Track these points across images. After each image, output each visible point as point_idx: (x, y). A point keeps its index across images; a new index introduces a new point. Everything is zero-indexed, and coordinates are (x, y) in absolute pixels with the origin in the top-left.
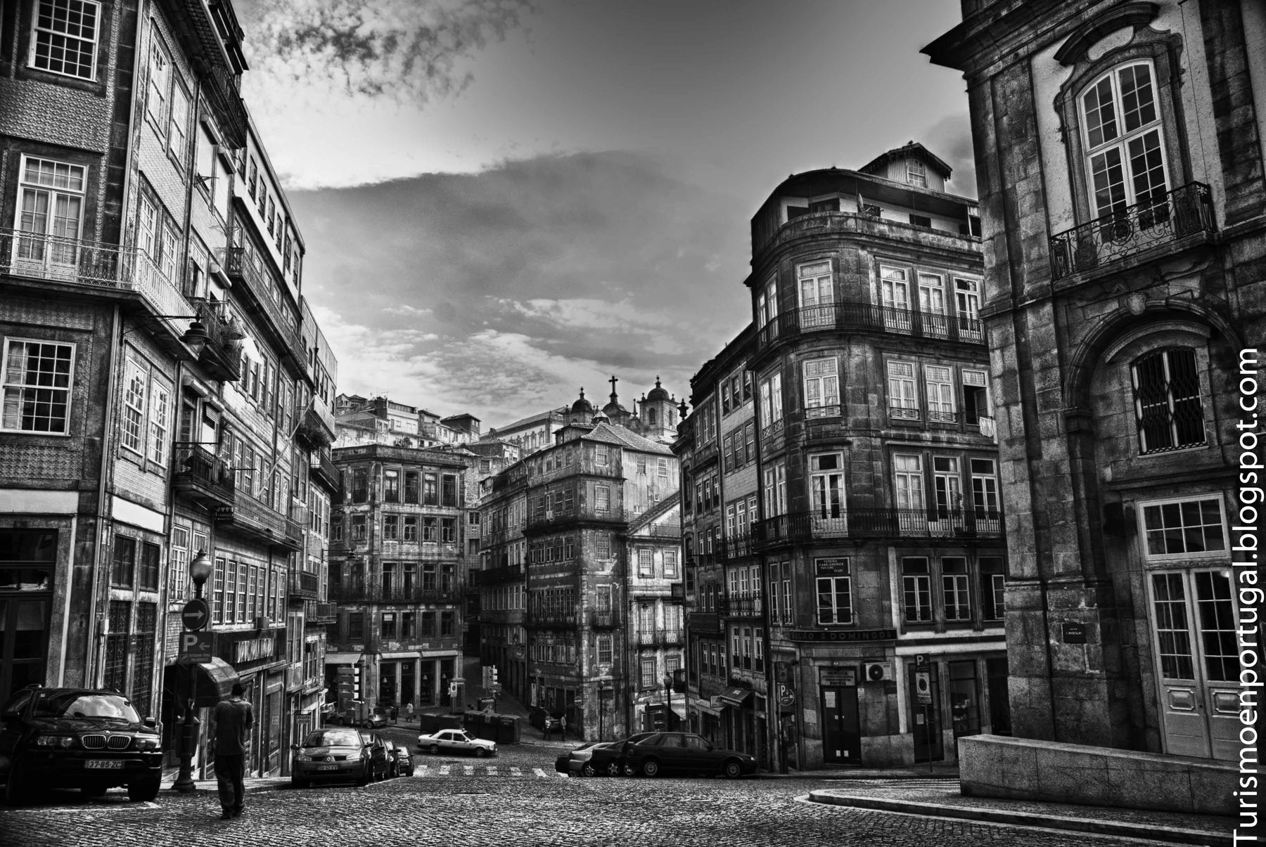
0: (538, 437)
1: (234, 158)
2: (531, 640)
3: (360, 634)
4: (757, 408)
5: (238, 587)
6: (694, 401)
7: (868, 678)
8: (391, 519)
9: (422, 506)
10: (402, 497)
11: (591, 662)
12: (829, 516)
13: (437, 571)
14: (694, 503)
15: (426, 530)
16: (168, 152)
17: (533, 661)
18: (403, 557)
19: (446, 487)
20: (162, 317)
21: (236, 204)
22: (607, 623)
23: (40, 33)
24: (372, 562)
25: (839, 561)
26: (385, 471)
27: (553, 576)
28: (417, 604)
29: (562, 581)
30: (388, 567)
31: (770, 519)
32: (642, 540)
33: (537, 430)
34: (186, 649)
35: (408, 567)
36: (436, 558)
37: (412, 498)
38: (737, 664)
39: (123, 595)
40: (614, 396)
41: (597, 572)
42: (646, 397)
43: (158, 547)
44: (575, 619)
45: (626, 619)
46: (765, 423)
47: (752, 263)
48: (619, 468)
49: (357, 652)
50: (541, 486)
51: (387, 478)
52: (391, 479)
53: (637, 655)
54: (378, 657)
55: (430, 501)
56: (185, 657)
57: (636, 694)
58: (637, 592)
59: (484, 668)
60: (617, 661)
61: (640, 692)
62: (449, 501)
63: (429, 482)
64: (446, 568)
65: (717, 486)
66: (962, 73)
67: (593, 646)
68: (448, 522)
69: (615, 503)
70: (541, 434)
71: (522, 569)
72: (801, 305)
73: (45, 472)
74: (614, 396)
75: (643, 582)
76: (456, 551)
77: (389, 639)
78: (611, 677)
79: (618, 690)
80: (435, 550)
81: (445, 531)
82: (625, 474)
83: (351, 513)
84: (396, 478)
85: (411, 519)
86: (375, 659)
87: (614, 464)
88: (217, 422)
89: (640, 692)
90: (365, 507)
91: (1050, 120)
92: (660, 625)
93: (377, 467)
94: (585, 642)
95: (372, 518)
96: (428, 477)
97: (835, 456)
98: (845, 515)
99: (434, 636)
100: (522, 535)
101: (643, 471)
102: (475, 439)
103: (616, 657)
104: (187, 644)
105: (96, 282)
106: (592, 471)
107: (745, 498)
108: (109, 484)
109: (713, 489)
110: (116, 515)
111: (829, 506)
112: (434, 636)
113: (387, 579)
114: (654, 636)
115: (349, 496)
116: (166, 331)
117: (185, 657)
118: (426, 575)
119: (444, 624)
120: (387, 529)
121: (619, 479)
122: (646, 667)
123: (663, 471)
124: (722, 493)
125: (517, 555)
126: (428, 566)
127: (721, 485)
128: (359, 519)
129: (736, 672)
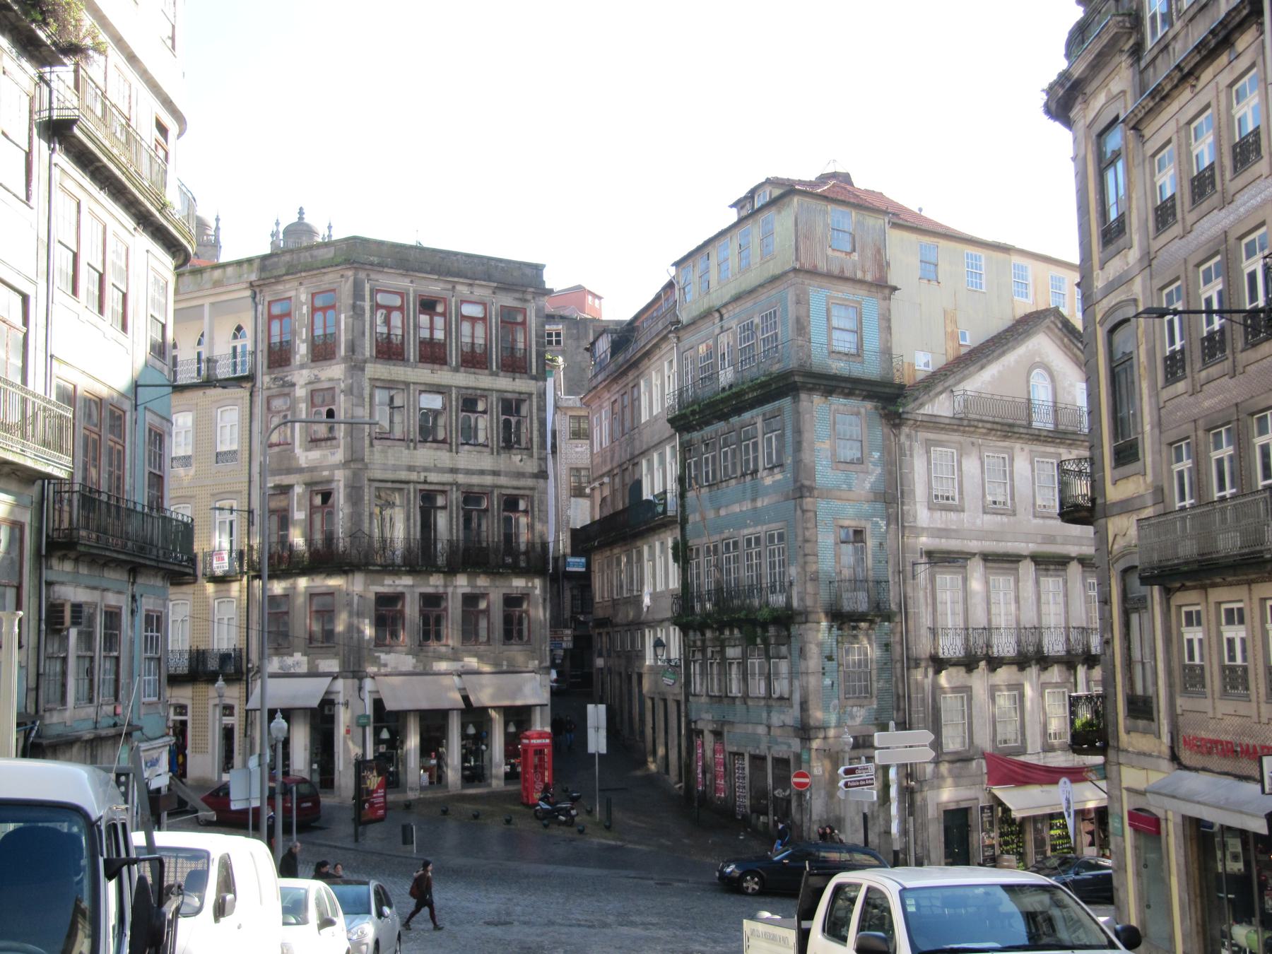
9: (456, 370)
10: (412, 352)
18: (414, 476)
22: (863, 607)
32: (934, 424)
36: (488, 480)
44: (789, 598)
48: (882, 265)
50: (706, 315)
54: (368, 684)
59: (590, 707)
63: (473, 320)
64: (511, 503)
68: (511, 406)
69: (872, 342)
75: (941, 519)
76: (531, 466)
81: (507, 424)
84: (401, 309)
86: (360, 689)
87: (869, 253)
90: (335, 371)
96: (468, 310)
100: (668, 430)
101: (930, 271)
106: (822, 266)
114: (967, 639)
119: (508, 620)
121: (883, 287)
126: (471, 497)
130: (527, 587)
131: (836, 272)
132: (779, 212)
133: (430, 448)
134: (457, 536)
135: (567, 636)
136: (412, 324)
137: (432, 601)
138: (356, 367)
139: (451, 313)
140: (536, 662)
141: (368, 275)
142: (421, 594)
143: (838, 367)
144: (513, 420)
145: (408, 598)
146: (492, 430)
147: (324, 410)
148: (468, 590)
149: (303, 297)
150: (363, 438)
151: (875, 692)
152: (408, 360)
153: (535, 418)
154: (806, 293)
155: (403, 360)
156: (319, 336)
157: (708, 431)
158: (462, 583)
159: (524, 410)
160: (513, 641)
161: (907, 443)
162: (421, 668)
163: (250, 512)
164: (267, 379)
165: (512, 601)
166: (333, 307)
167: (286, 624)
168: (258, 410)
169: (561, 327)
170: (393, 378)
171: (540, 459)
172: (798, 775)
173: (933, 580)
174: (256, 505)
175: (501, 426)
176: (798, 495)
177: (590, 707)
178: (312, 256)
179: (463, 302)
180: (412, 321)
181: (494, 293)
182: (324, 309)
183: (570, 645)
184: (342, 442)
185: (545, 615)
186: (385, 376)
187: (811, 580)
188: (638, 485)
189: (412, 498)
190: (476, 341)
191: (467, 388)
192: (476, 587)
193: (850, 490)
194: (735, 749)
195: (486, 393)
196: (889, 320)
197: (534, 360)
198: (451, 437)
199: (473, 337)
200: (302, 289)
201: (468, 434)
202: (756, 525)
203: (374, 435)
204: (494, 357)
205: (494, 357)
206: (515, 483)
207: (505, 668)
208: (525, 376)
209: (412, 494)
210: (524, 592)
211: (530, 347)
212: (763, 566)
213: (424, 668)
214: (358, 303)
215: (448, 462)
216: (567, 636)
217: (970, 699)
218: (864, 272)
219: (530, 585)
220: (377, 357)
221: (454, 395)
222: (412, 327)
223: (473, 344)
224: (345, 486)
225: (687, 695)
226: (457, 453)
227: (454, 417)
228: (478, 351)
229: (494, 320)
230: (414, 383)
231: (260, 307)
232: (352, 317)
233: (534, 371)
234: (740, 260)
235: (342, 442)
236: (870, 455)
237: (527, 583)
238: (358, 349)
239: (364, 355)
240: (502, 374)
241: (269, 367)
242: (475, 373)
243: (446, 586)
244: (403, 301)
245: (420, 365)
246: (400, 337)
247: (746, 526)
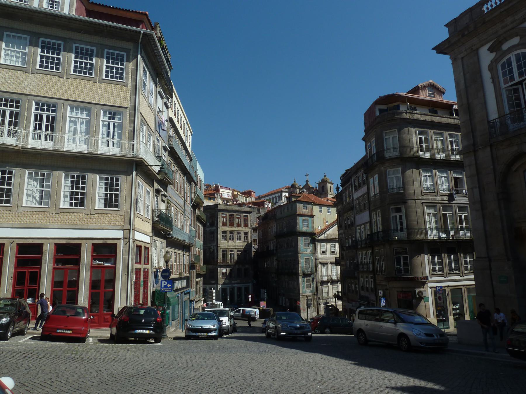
0: (277, 198)
1: (169, 102)
4: (368, 188)
5: (177, 262)
6: (342, 185)
7: (417, 296)
8: (224, 233)
11: (303, 288)
12: (399, 231)
14: (343, 226)
16: (150, 106)
18: (229, 247)
19: (244, 220)
20: (150, 166)
21: (171, 120)
22: (309, 273)
23: (106, 66)
25: (404, 249)
31: (375, 233)
33: (277, 195)
34: (163, 287)
35: (231, 251)
37: (232, 224)
38: (363, 289)
39: (138, 266)
40: (307, 181)
42: (320, 181)
43: (148, 248)
46: (372, 194)
47: (365, 131)
48: (312, 212)
52: (223, 217)
55: (239, 225)
56: (163, 289)
57: (321, 300)
58: (320, 260)
59: (261, 290)
60: (313, 287)
61: (323, 300)
62: (246, 225)
63: (238, 218)
65: (352, 219)
66: (449, 56)
67: (303, 281)
68: (246, 233)
69: (310, 225)
70: (279, 197)
71: (275, 251)
72: (385, 148)
73: (113, 222)
74: (307, 181)
78: (311, 294)
79: (314, 299)
83: (209, 230)
85: (231, 233)
87: (310, 210)
88: (166, 201)
89: (323, 300)
91: (487, 75)
92: (330, 273)
94: (300, 280)
97: (401, 207)
98: (406, 231)
101: (321, 211)
102: (253, 199)
103: (313, 286)
104: (163, 285)
105: (127, 154)
106: (302, 213)
107: (364, 224)
108: (134, 226)
109: (351, 220)
110: (136, 238)
111: (399, 227)
114: (328, 277)
115: (208, 224)
116: (150, 170)
117: (163, 289)
120: (223, 236)
121: (312, 216)
122: (325, 290)
123: (329, 212)
124: (355, 222)
125: (272, 245)
127: (354, 218)
129: (363, 293)
131: (304, 214)
147: (212, 235)
173: (321, 267)
177: (261, 290)
188: (268, 247)
217: (328, 288)
218: (309, 213)
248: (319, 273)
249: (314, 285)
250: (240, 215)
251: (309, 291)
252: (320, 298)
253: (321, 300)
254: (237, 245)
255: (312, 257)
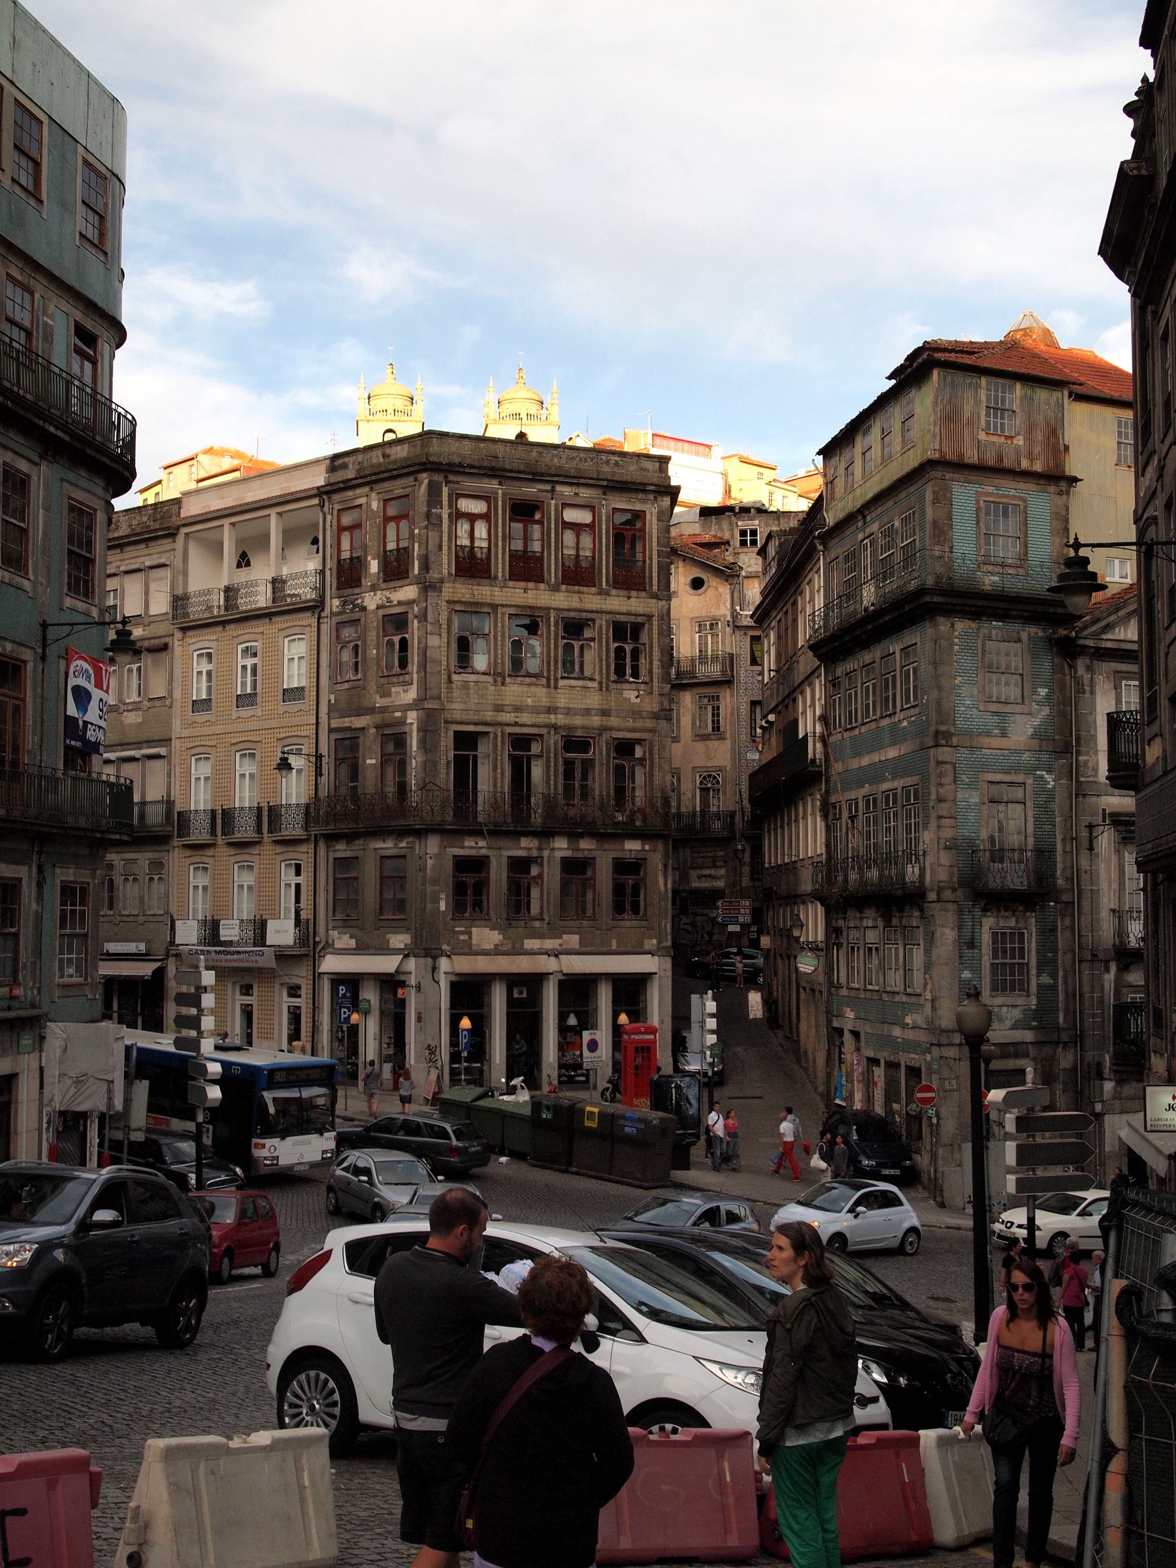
2: (834, 931)
3: (400, 905)
9: (555, 589)
10: (500, 566)
13: (600, 753)
15: (568, 648)
17: (840, 986)
24: (428, 729)
26: (455, 497)
27: (875, 757)
28: (545, 834)
29: (897, 768)
30: (466, 741)
35: (521, 742)
36: (596, 721)
41: (985, 741)
44: (922, 871)
45: (1075, 876)
48: (1057, 448)
49: (395, 952)
51: (457, 515)
52: (472, 518)
53: (1110, 978)
57: (1108, 1086)
60: (1046, 992)
63: (576, 527)
64: (624, 748)
67: (972, 944)
77: (473, 921)
78: (1028, 1036)
80: (594, 700)
81: (620, 653)
82: (1073, 467)
83: (379, 607)
84: (485, 517)
86: (434, 969)
87: (1039, 436)
90: (409, 592)
93: (434, 492)
95: (423, 617)
96: (571, 515)
99: (593, 918)
103: (1046, 980)
112: (593, 918)
113: (464, 770)
115: (374, 566)
118: (569, 764)
119: (618, 890)
126: (575, 743)
128: (397, 622)
130: (643, 850)
132: (920, 388)
133: (522, 684)
134: (556, 788)
135: (745, 907)
136: (500, 534)
137: (519, 866)
138: (428, 587)
139: (549, 519)
140: (655, 941)
141: (446, 477)
142: (509, 857)
143: (989, 581)
144: (628, 648)
145: (494, 863)
146: (601, 660)
147: (396, 639)
148: (568, 853)
149: (375, 505)
150: (440, 672)
151: (1033, 988)
152: (496, 578)
153: (655, 645)
154: (948, 490)
155: (489, 577)
156: (391, 551)
157: (850, 665)
158: (561, 846)
159: (644, 638)
160: (625, 916)
161: (1087, 677)
162: (510, 946)
163: (319, 757)
164: (336, 602)
165: (627, 868)
166: (405, 516)
167: (356, 891)
168: (325, 640)
169: (757, 522)
170: (478, 598)
171: (661, 695)
172: (921, 1091)
174: (324, 750)
175: (612, 655)
176: (931, 743)
177: (693, 997)
178: (384, 456)
179: (565, 505)
180: (500, 530)
181: (604, 493)
182: (397, 519)
183: (748, 919)
184: (415, 676)
185: (666, 884)
186: (467, 598)
187: (946, 848)
189: (499, 744)
190: (581, 553)
191: (568, 610)
192: (578, 850)
193: (1004, 734)
194: (871, 1054)
195: (593, 616)
196: (1067, 521)
197: (655, 574)
198: (549, 671)
199: (578, 548)
200: (373, 495)
201: (570, 667)
202: (893, 779)
203: (453, 670)
204: (604, 571)
205: (604, 571)
206: (630, 723)
207: (614, 947)
208: (643, 594)
209: (499, 739)
210: (640, 856)
211: (651, 559)
212: (900, 830)
213: (514, 947)
214: (434, 511)
215: (544, 700)
216: (745, 907)
218: (1031, 459)
219: (647, 847)
220: (456, 575)
221: (552, 619)
222: (500, 539)
223: (578, 556)
224: (419, 730)
225: (830, 983)
226: (556, 688)
227: (552, 646)
228: (584, 565)
229: (604, 527)
230: (502, 606)
231: (329, 517)
232: (426, 527)
233: (655, 588)
234: (883, 447)
235: (415, 676)
236: (1034, 692)
237: (643, 845)
238: (433, 566)
239: (440, 573)
240: (614, 592)
241: (338, 589)
242: (579, 592)
243: (540, 849)
244: (489, 507)
245: (511, 583)
246: (485, 550)
247: (885, 780)
248: (1095, 894)
249: (1054, 975)
250: (591, 508)
251: (1017, 1013)
252: (1099, 1065)
253: (1108, 1086)
254: (562, 701)
255: (1049, 778)
